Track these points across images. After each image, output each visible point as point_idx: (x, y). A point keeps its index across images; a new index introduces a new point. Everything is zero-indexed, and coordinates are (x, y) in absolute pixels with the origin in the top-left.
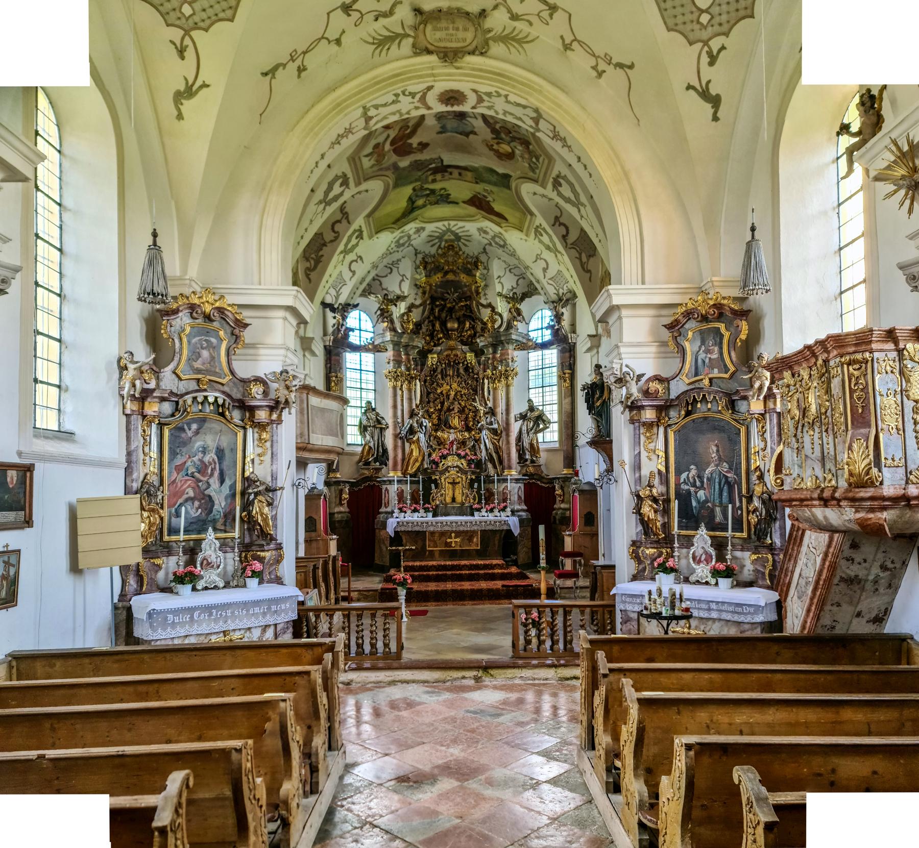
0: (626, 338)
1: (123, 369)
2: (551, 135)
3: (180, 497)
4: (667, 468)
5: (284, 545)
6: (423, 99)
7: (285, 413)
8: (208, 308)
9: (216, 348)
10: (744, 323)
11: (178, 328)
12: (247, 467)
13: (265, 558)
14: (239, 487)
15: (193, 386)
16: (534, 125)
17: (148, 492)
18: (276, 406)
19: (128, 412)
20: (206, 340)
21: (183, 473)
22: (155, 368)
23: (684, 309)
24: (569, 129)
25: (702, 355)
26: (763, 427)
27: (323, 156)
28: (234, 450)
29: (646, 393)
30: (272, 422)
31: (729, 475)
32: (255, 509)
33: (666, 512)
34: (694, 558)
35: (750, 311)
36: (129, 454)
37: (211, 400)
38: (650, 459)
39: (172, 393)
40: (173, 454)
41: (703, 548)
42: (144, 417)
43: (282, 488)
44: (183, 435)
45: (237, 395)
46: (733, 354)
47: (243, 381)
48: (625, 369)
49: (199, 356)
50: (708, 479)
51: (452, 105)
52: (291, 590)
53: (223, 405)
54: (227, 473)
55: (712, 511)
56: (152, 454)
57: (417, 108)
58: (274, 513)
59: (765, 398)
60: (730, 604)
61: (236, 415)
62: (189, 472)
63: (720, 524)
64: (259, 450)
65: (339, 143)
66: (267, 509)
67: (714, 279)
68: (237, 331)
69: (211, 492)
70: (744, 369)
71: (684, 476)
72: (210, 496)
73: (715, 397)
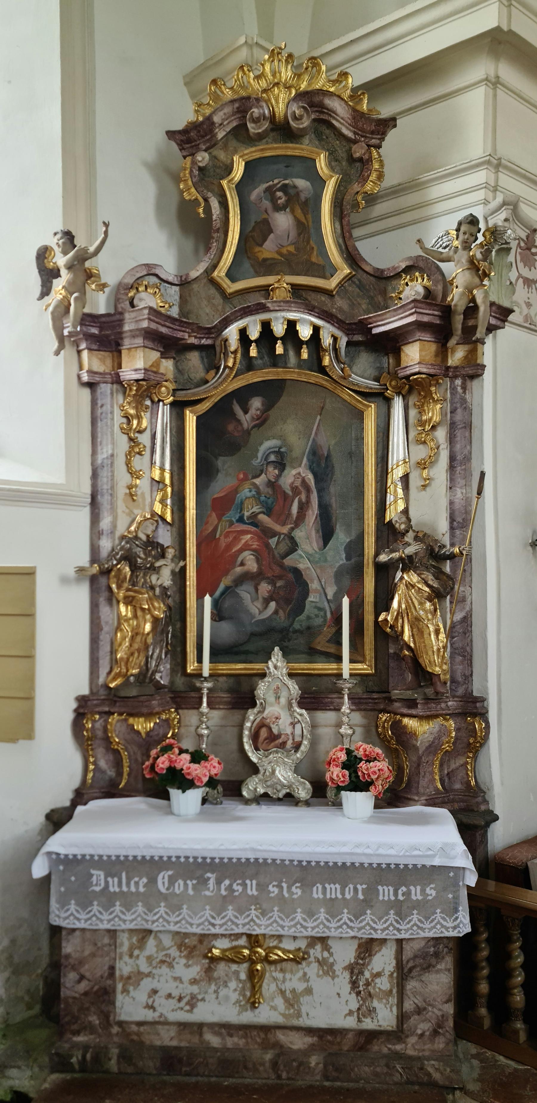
20: (284, 188)
62: (246, 514)
64: (420, 452)
72: (297, 572)
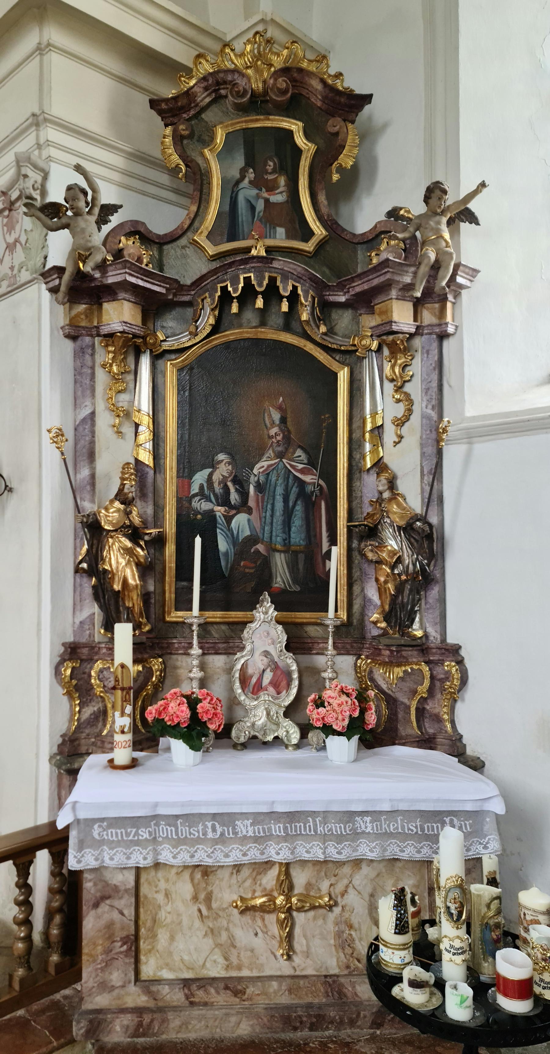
25: (247, 192)
26: (404, 367)
31: (308, 478)
34: (244, 681)
38: (119, 433)
41: (266, 654)
60: (409, 814)
71: (200, 478)
73: (295, 288)
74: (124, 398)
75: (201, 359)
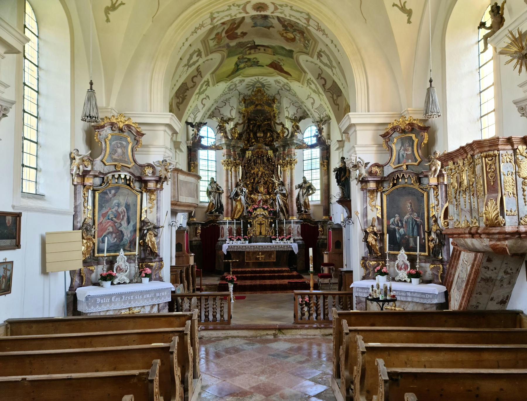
0: (359, 143)
1: (73, 159)
2: (316, 28)
3: (105, 232)
4: (382, 215)
5: (164, 259)
6: (244, 9)
7: (165, 184)
8: (121, 125)
9: (126, 147)
10: (426, 133)
11: (104, 136)
12: (143, 215)
13: (152, 266)
14: (138, 226)
15: (112, 168)
16: (306, 22)
17: (86, 229)
18: (160, 180)
19: (75, 183)
20: (120, 143)
21: (107, 218)
22: (91, 159)
23: (392, 126)
24: (326, 24)
25: (402, 152)
26: (437, 193)
27: (187, 40)
28: (135, 205)
29: (370, 173)
30: (157, 189)
31: (417, 220)
32: (147, 239)
33: (382, 240)
34: (398, 267)
35: (429, 127)
36: (76, 207)
37: (123, 176)
39: (100, 173)
40: (101, 207)
42: (84, 186)
43: (163, 227)
44: (107, 197)
45: (138, 174)
46: (420, 151)
47: (141, 166)
48: (358, 160)
49: (116, 151)
50: (405, 222)
51: (260, 11)
52: (167, 285)
53: (129, 180)
54: (132, 218)
55: (408, 241)
56: (89, 207)
57: (240, 13)
58: (158, 241)
59: (438, 176)
61: (137, 185)
62: (110, 218)
63: (412, 247)
64: (150, 205)
65: (196, 32)
66: (154, 238)
67: (409, 109)
68: (137, 138)
69: (122, 229)
70: (426, 160)
71: (392, 220)
72: (121, 231)
74: (373, 203)
75: (392, 192)
